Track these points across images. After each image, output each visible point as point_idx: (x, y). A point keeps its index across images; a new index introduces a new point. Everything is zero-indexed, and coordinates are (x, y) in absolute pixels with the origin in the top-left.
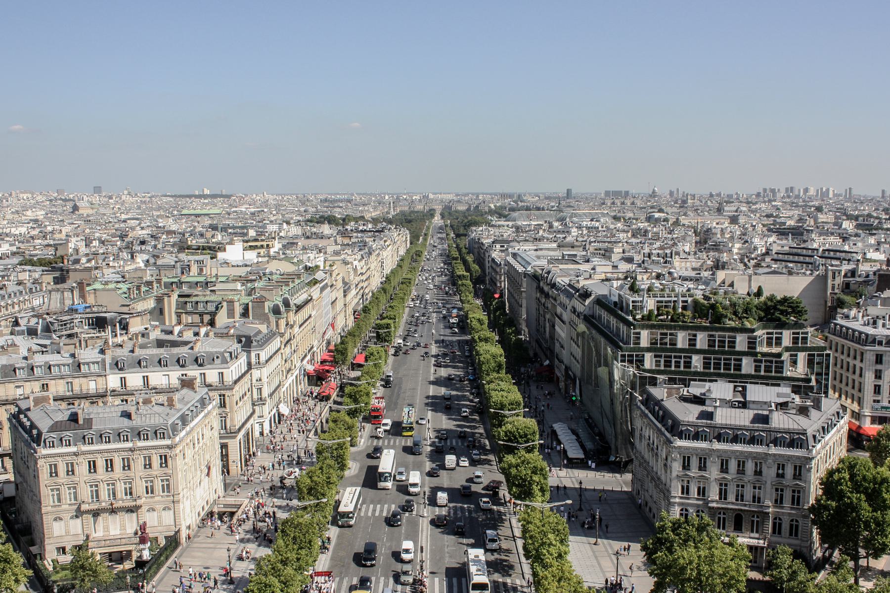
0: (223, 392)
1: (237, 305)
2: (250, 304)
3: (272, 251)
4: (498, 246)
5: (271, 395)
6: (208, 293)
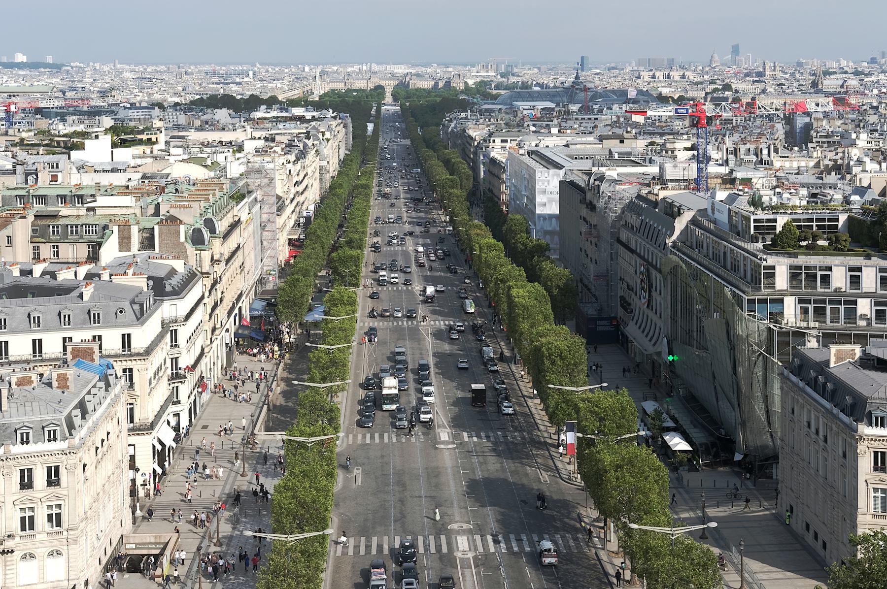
0: (129, 364)
1: (135, 230)
2: (157, 228)
3: (156, 147)
4: (498, 140)
5: (193, 368)
6: (83, 212)
